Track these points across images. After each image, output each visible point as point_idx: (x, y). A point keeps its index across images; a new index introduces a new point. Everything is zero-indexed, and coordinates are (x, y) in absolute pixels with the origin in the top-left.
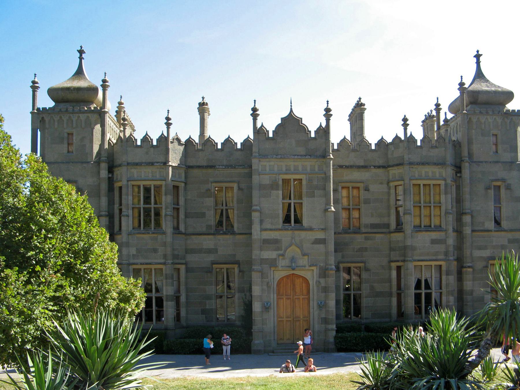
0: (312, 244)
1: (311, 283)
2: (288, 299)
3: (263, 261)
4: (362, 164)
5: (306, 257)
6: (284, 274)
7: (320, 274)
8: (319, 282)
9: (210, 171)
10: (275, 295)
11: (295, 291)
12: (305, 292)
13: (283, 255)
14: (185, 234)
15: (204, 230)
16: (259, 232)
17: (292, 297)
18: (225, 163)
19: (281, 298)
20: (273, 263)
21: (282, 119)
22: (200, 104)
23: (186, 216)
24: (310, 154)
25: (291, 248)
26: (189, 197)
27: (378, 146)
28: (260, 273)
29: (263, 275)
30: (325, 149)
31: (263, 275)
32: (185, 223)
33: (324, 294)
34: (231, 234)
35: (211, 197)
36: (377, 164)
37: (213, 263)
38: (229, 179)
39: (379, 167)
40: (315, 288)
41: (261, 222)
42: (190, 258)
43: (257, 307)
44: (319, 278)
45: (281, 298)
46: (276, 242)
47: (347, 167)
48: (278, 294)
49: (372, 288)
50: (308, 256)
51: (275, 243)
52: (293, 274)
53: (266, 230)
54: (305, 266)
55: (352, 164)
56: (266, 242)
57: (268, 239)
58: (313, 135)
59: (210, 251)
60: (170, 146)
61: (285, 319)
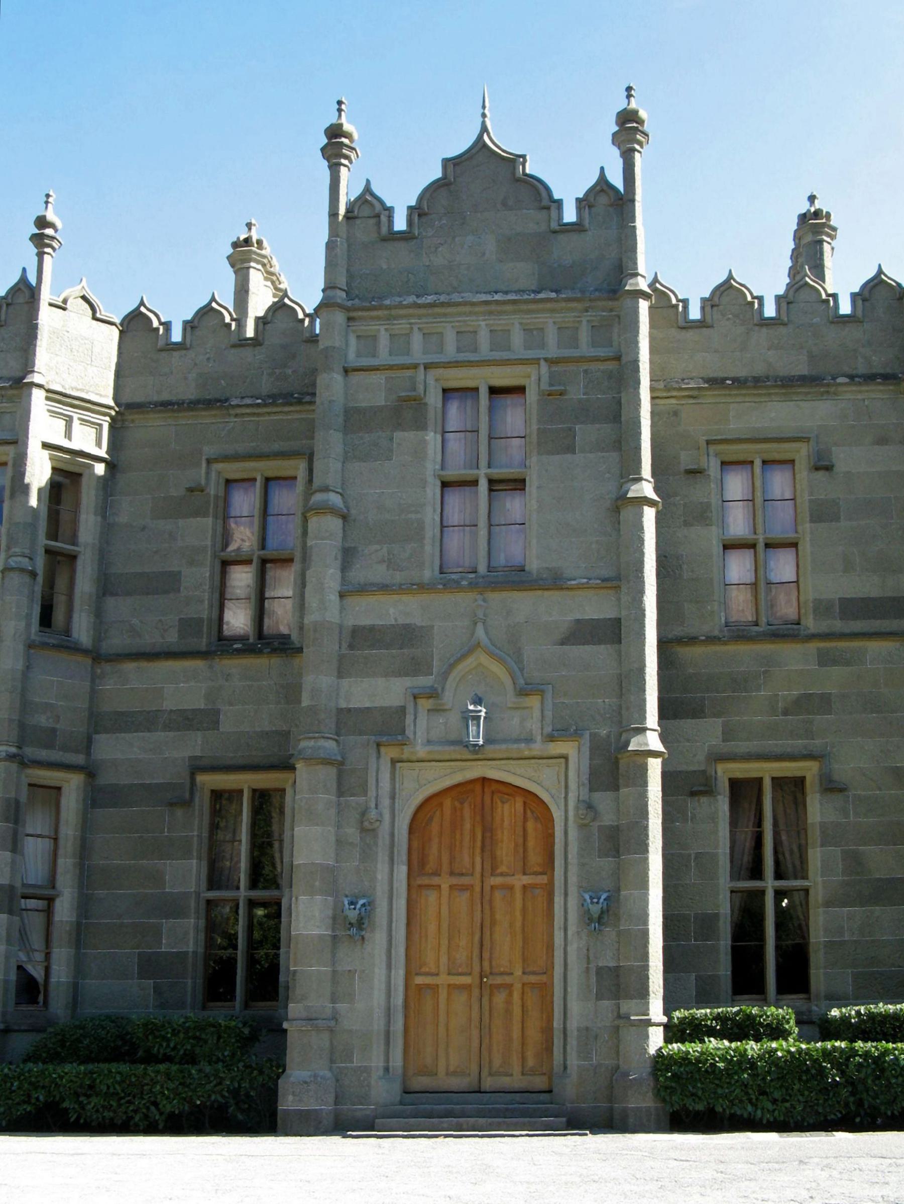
0: (562, 643)
1: (557, 815)
2: (463, 888)
3: (348, 720)
4: (802, 368)
5: (534, 702)
6: (440, 778)
7: (594, 774)
8: (590, 807)
9: (206, 418)
10: (402, 871)
11: (493, 857)
12: (535, 858)
13: (433, 694)
14: (97, 656)
15: (172, 638)
16: (334, 598)
17: (476, 881)
18: (266, 386)
19: (428, 886)
20: (388, 728)
21: (446, 162)
22: (235, 245)
23: (106, 586)
24: (558, 282)
25: (470, 662)
26: (123, 519)
27: (864, 300)
28: (333, 771)
29: (347, 781)
30: (621, 260)
31: (347, 781)
32: (98, 613)
33: (607, 863)
34: (274, 651)
35: (205, 515)
36: (862, 369)
37: (197, 767)
38: (276, 447)
39: (870, 378)
40: (573, 833)
41: (348, 556)
42: (117, 751)
43: (307, 917)
44: (591, 790)
45: (428, 886)
46: (407, 636)
47: (739, 383)
48: (418, 865)
49: (854, 862)
50: (542, 693)
51: (401, 645)
52: (484, 780)
53: (363, 589)
54: (529, 740)
55: (759, 369)
56: (362, 638)
57: (372, 629)
58: (570, 215)
59: (188, 721)
60: (46, 317)
61: (443, 979)
